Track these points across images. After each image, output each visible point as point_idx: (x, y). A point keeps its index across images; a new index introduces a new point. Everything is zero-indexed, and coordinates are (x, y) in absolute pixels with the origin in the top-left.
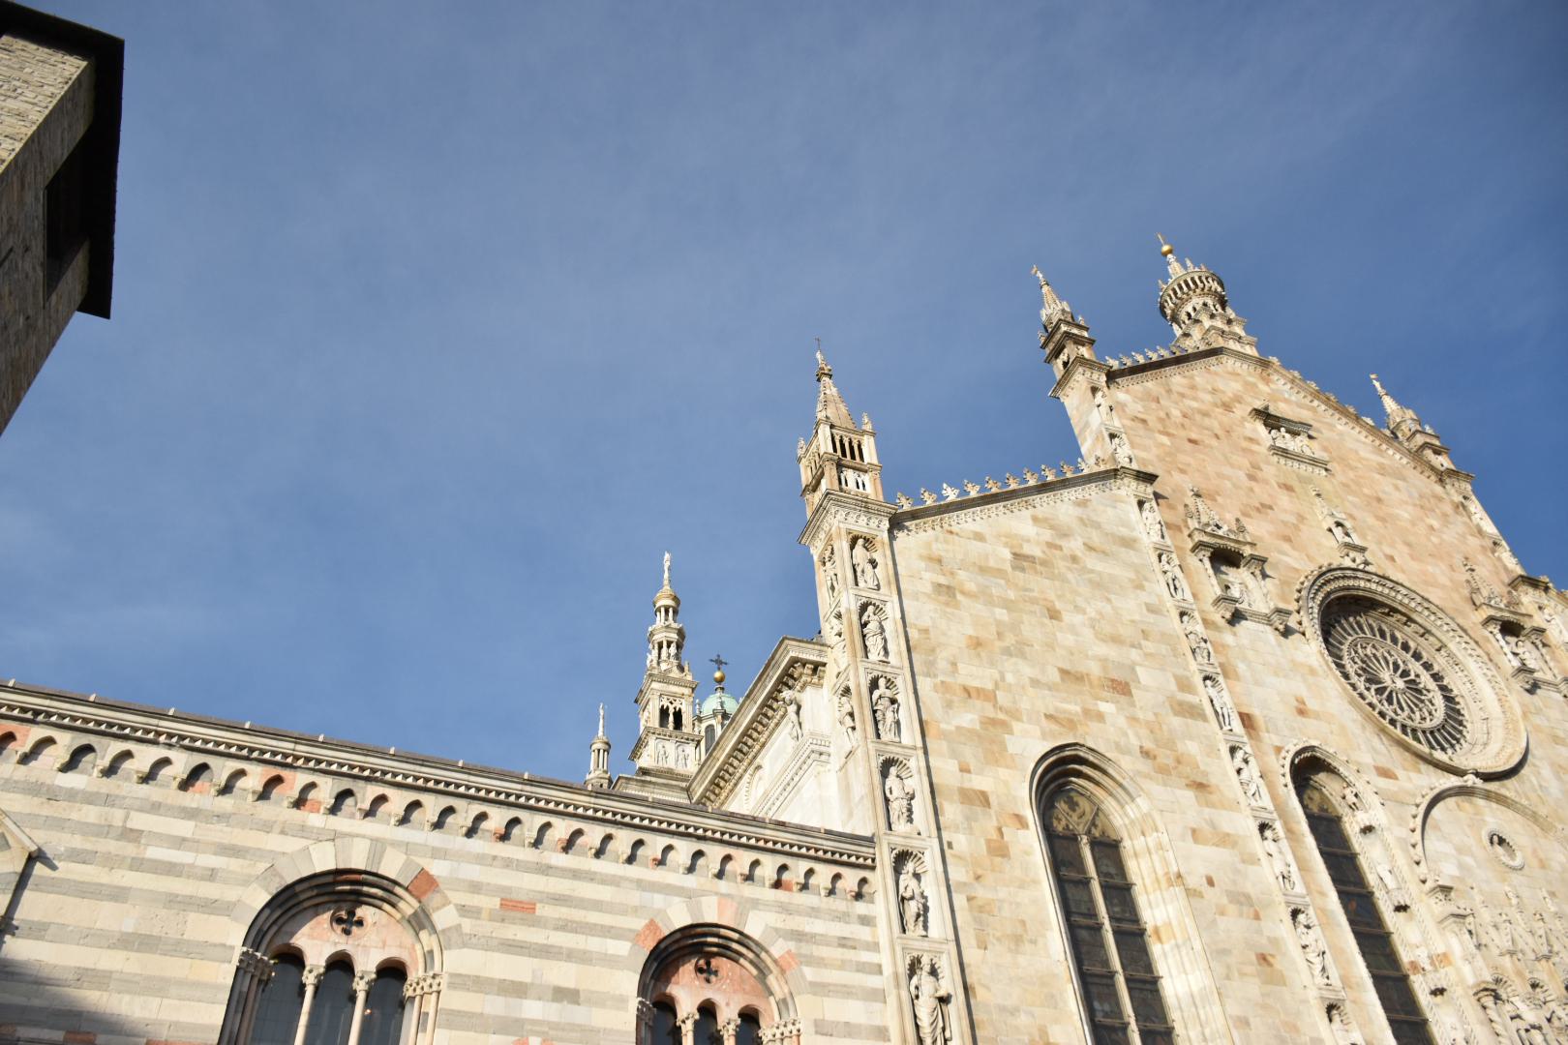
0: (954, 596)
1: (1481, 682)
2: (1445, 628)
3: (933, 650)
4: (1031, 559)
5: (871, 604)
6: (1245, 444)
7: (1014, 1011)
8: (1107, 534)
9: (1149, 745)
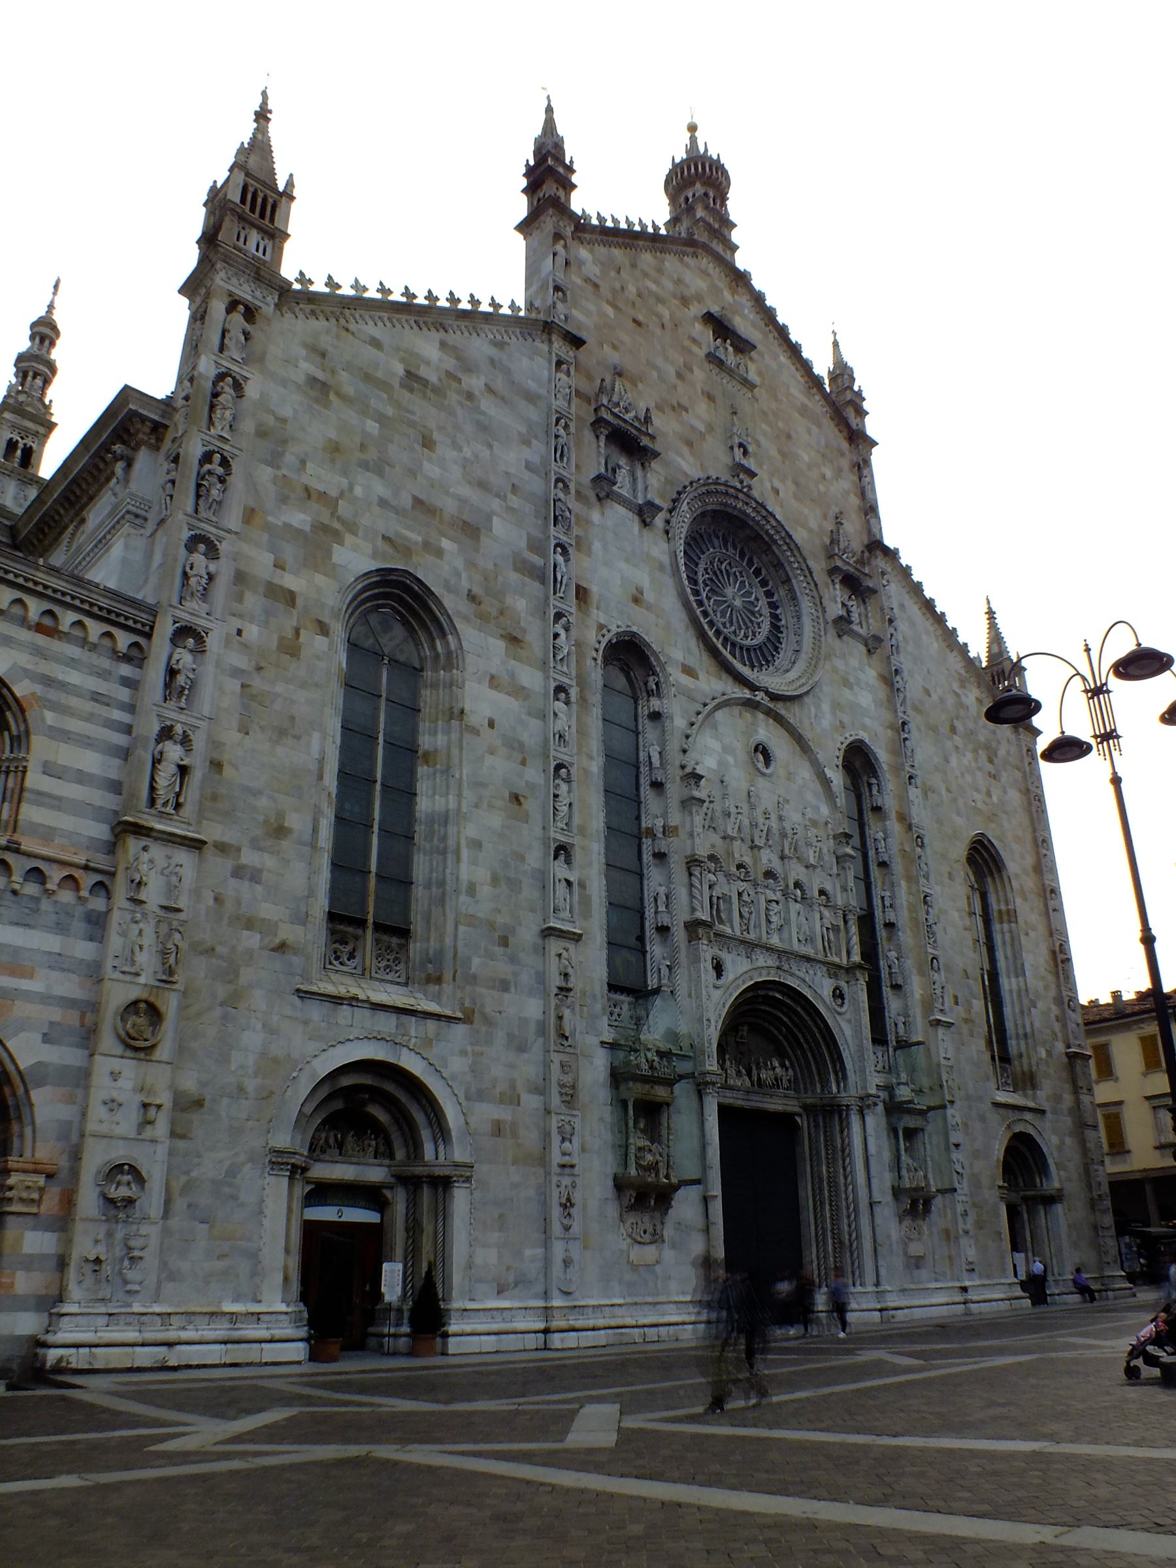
0: (327, 395)
1: (807, 622)
2: (796, 565)
3: (285, 442)
4: (425, 383)
5: (230, 376)
6: (687, 343)
7: (256, 793)
8: (513, 383)
9: (477, 590)
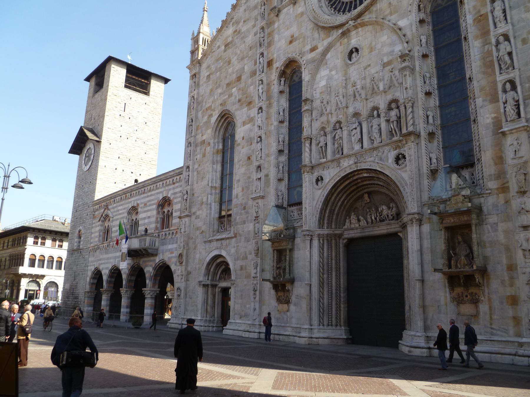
3: (203, 101)
9: (241, 96)
